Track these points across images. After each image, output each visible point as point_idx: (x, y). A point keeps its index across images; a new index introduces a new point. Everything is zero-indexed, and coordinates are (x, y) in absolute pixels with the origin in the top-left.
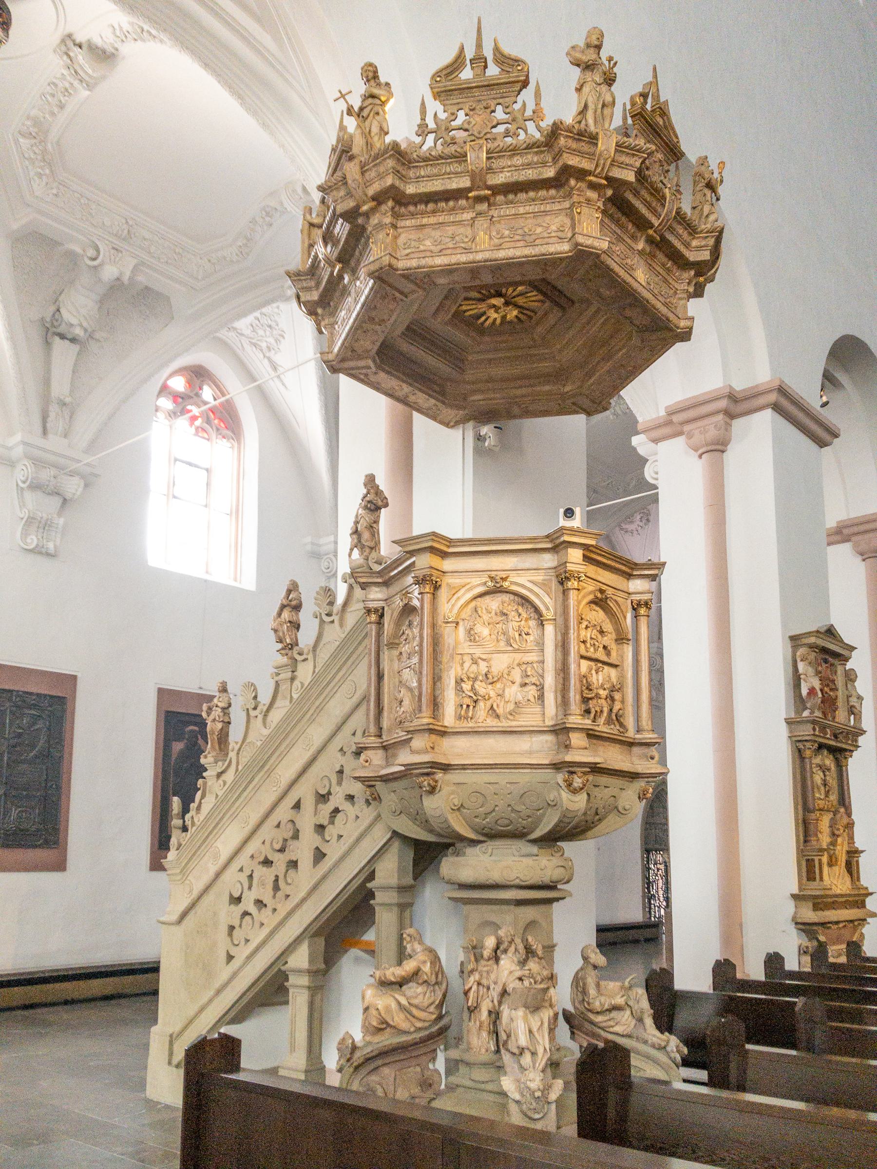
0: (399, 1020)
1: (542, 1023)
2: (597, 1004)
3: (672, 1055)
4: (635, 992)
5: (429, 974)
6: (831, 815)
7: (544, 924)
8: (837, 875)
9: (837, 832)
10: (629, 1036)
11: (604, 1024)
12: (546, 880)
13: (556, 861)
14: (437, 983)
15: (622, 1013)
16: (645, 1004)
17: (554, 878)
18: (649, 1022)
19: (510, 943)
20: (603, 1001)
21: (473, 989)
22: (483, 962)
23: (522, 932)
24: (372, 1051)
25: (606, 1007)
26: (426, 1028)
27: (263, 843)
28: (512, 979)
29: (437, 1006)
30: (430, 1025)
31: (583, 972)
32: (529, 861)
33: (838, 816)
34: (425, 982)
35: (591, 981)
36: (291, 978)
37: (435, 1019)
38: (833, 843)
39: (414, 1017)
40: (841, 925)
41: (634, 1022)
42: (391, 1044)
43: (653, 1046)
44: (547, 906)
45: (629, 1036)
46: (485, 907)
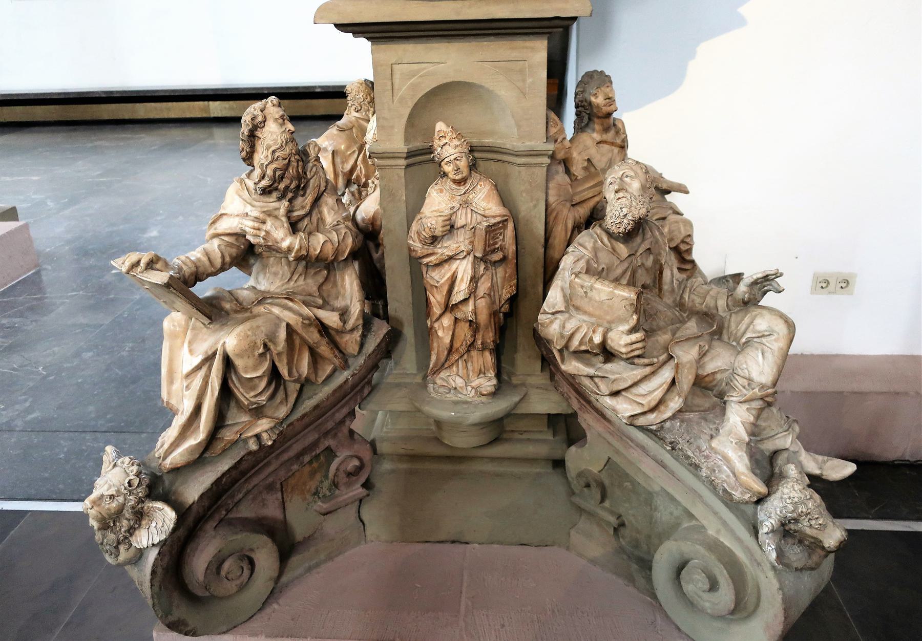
43: (712, 485)
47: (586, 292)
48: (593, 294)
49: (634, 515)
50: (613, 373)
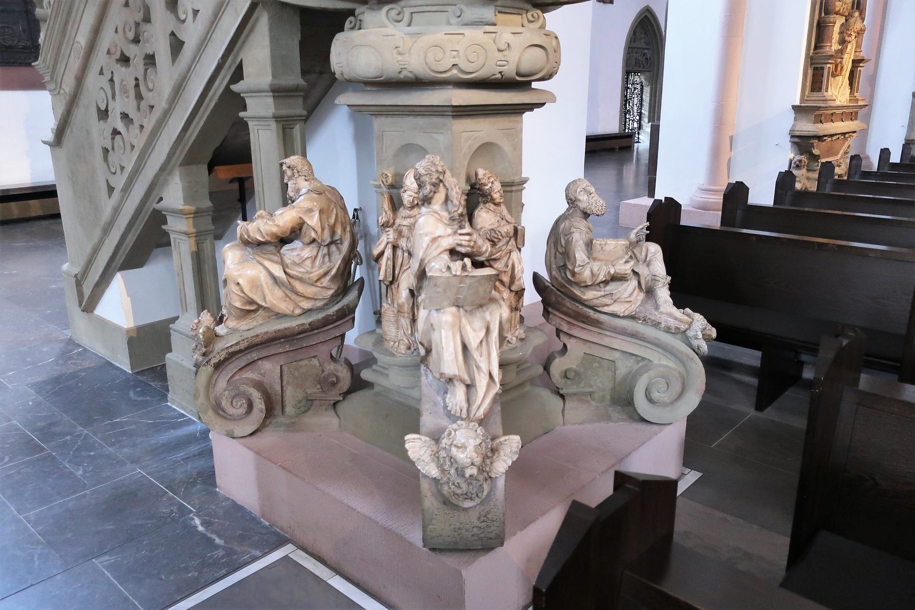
0: (274, 298)
1: (488, 331)
2: (587, 273)
3: (695, 343)
4: (644, 249)
5: (319, 231)
6: (843, 20)
7: (507, 147)
8: (840, 84)
9: (847, 38)
10: (632, 317)
11: (596, 302)
12: (510, 70)
13: (530, 35)
14: (333, 242)
15: (625, 285)
16: (659, 267)
17: (525, 67)
18: (664, 294)
19: (435, 185)
20: (595, 269)
21: (386, 255)
22: (403, 212)
23: (466, 163)
24: (237, 344)
25: (601, 278)
26: (320, 309)
27: (116, 31)
28: (435, 253)
29: (335, 277)
30: (326, 305)
31: (567, 222)
32: (476, 34)
33: (852, 20)
34: (314, 240)
35: (578, 239)
36: (169, 219)
37: (333, 296)
38: (841, 52)
39: (297, 293)
40: (834, 138)
41: (642, 296)
42: (266, 333)
43: (668, 330)
44: (514, 118)
45: (632, 317)
46: (410, 121)
47: (602, 248)
48: (607, 248)
49: (600, 382)
50: (614, 290)
